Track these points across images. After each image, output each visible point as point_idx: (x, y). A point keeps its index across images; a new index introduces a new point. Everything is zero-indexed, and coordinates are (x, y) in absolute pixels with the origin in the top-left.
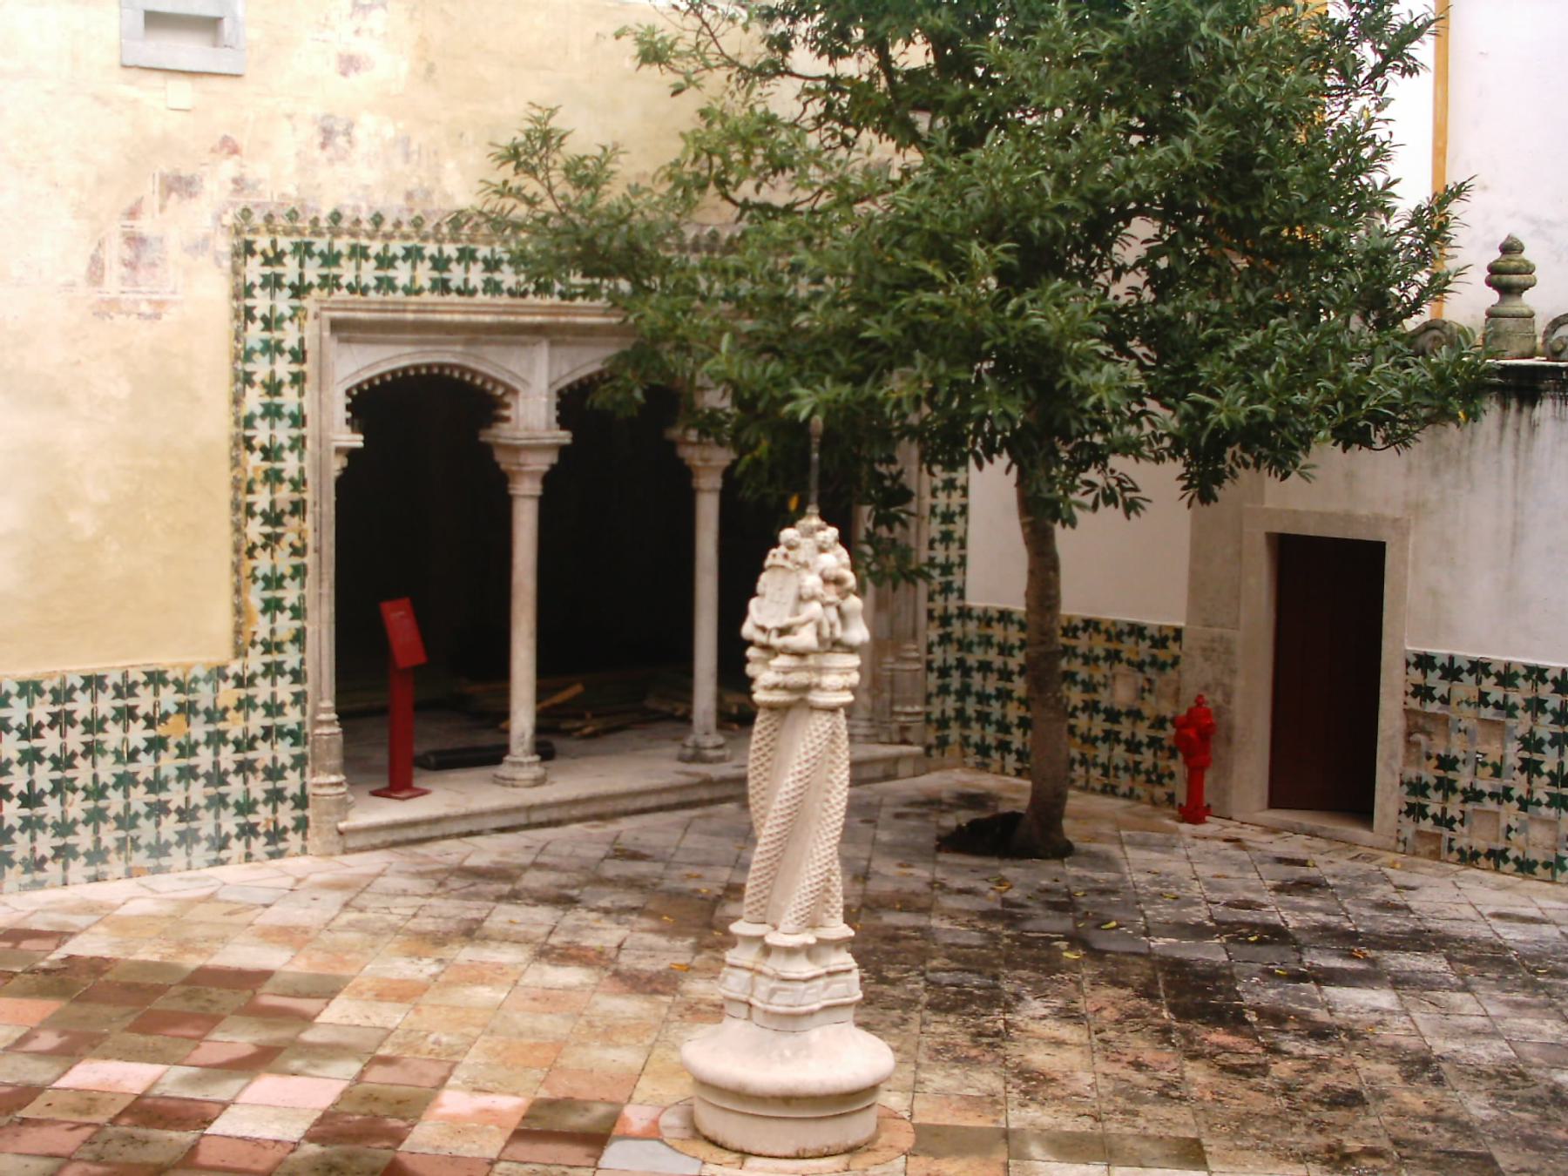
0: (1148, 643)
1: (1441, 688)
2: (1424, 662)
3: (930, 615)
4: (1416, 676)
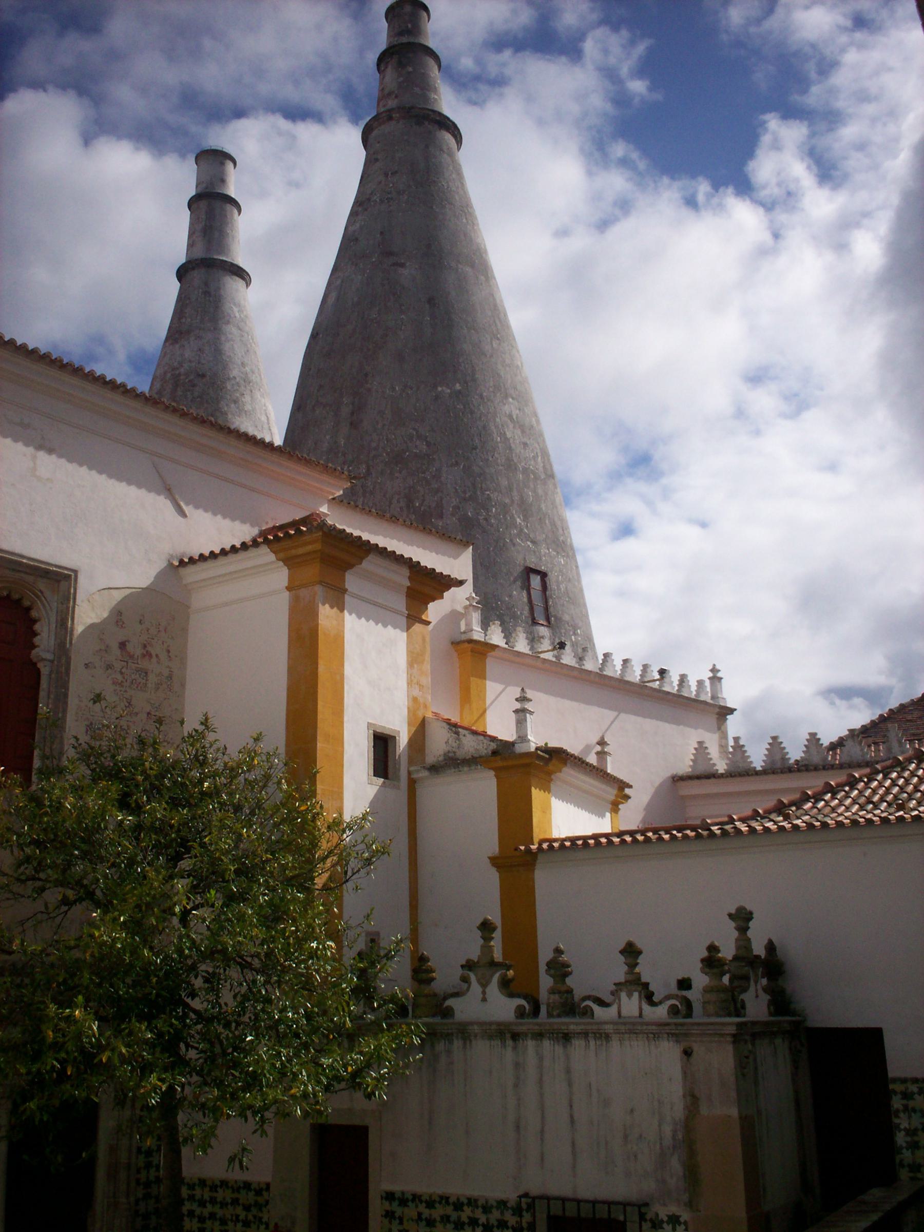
0: (253, 1193)
1: (399, 1211)
2: (389, 1196)
3: (138, 1182)
4: (387, 1205)
